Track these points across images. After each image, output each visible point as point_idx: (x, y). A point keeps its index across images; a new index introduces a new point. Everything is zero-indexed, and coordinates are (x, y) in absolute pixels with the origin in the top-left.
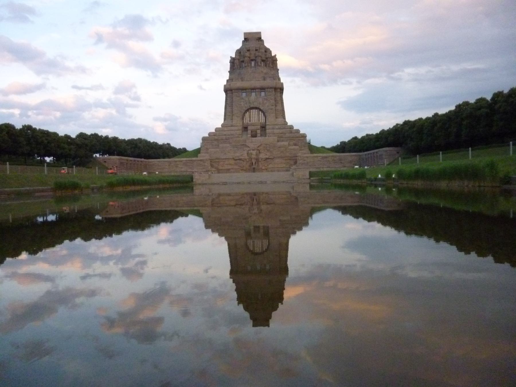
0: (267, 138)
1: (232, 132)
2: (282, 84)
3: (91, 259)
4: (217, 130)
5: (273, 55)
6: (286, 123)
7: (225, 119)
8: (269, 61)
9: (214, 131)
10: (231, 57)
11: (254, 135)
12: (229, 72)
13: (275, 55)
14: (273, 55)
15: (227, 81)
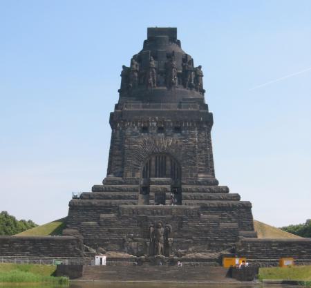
0: (183, 206)
1: (122, 194)
2: (211, 115)
3: (286, 238)
4: (95, 188)
5: (196, 65)
6: (216, 183)
7: (110, 171)
8: (191, 76)
9: (89, 190)
10: (124, 67)
11: (161, 198)
12: (119, 91)
13: (200, 67)
14: (196, 65)
15: (117, 107)
